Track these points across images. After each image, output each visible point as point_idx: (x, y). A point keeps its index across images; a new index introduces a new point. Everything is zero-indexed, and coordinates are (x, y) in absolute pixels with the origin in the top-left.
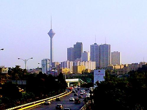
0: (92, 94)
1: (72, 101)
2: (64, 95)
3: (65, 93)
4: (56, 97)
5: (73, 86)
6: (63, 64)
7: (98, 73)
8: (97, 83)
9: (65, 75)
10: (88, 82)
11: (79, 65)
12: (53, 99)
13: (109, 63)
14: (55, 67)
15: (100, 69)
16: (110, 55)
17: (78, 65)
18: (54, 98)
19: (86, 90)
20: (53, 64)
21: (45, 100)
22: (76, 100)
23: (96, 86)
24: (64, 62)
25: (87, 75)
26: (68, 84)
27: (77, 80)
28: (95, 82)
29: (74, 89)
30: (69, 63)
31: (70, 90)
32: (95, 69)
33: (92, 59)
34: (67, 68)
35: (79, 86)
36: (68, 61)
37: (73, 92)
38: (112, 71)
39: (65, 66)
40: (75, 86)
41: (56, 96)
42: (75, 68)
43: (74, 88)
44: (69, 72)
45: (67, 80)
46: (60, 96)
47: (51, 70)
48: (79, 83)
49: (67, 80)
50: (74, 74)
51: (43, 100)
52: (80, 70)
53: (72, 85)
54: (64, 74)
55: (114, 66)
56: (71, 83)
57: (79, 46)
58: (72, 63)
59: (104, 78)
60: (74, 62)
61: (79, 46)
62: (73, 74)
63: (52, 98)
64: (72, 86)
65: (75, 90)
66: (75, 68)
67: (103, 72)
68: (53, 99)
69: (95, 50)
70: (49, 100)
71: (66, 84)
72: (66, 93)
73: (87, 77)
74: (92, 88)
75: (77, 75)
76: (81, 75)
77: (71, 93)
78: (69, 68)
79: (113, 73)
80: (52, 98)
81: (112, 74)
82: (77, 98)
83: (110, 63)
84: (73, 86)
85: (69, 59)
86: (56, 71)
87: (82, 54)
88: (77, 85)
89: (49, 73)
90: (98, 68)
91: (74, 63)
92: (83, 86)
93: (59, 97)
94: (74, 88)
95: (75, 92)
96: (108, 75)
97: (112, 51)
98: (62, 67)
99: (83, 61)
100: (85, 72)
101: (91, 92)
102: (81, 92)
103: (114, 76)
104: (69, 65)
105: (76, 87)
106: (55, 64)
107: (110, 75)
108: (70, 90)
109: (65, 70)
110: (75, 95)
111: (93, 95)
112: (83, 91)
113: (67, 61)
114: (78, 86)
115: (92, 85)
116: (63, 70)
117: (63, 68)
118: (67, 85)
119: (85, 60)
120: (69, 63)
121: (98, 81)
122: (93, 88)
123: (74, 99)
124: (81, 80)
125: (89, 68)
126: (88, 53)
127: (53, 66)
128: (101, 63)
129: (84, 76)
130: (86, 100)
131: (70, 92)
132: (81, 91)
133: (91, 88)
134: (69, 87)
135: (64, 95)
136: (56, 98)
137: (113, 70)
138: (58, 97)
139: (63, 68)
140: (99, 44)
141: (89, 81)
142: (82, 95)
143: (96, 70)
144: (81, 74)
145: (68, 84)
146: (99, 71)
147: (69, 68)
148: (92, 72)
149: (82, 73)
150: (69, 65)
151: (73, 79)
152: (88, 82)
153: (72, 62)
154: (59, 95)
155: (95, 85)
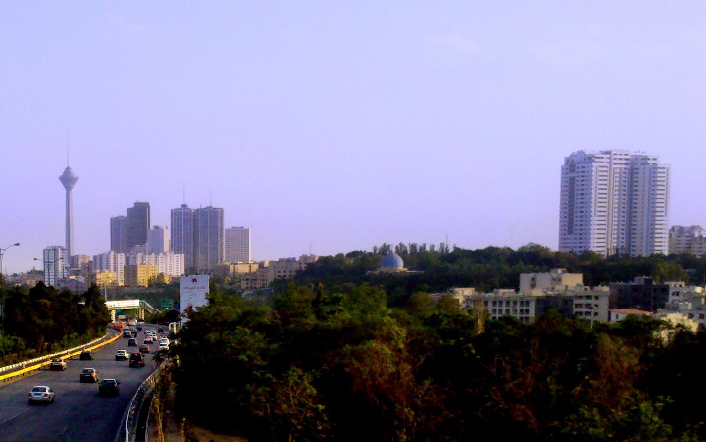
0: (176, 342)
1: (124, 358)
2: (101, 345)
3: (104, 337)
4: (82, 349)
5: (126, 320)
6: (100, 261)
7: (192, 284)
8: (189, 310)
9: (104, 290)
10: (164, 308)
11: (142, 264)
12: (74, 354)
13: (219, 257)
14: (78, 267)
15: (196, 274)
16: (221, 237)
17: (138, 264)
18: (74, 352)
19: (160, 331)
20: (73, 260)
21: (51, 358)
22: (132, 356)
23: (184, 320)
24: (101, 256)
25: (161, 291)
26: (113, 313)
27: (136, 303)
28: (183, 307)
29: (127, 327)
30: (115, 258)
31: (118, 329)
32: (183, 272)
33: (176, 248)
34: (110, 272)
35: (142, 321)
36: (112, 253)
37: (126, 336)
38: (228, 280)
39: (104, 265)
40: (131, 319)
41: (82, 346)
42: (131, 271)
43: (129, 325)
44: (114, 283)
45: (109, 304)
46: (92, 346)
47: (69, 275)
48: (140, 311)
49: (109, 304)
50: (128, 286)
51: (45, 357)
52: (143, 277)
53: (123, 317)
54: (101, 288)
55: (232, 267)
56: (123, 312)
57: (140, 212)
58: (121, 259)
59: (208, 299)
60: (128, 255)
61: (140, 212)
62: (125, 286)
63: (71, 353)
64: (122, 320)
65: (130, 329)
66: (131, 271)
67: (204, 281)
68: (74, 354)
69: (184, 222)
70: (63, 358)
71: (106, 312)
72: (107, 339)
73: (163, 295)
74: (174, 324)
75: (136, 290)
76: (147, 289)
77: (120, 338)
78: (115, 270)
79: (231, 284)
80: (71, 353)
81: (227, 287)
82: (136, 351)
83: (221, 258)
84: (126, 320)
85: (116, 246)
86: (81, 279)
87: (149, 234)
88: (137, 316)
89: (62, 285)
90: (191, 270)
91: (127, 259)
92: (153, 320)
93: (89, 349)
94: (129, 325)
95: (129, 337)
96: (218, 289)
97: (228, 223)
98: (96, 269)
99: (152, 252)
100: (157, 282)
101: (172, 337)
102: (146, 335)
103: (232, 292)
104: (115, 263)
105: (134, 322)
106: (79, 260)
107: (222, 289)
108: (118, 329)
109: (107, 277)
110: (131, 344)
111: (178, 344)
112: (152, 333)
113: (109, 253)
114: (140, 320)
115: (173, 316)
116: (98, 276)
117: (98, 271)
118: (111, 316)
119: (157, 250)
120: (115, 258)
121: (191, 307)
122: (177, 325)
123: (127, 355)
124: (146, 303)
125: (169, 270)
126: (165, 230)
127: (73, 266)
128: (200, 256)
129: (153, 291)
130: (159, 357)
131: (118, 337)
132: (145, 333)
133: (172, 326)
134: (114, 321)
135: (101, 345)
136: (79, 353)
137: (229, 276)
138: (86, 350)
139: (98, 271)
140: (193, 206)
141: (168, 307)
142: (150, 343)
143: (187, 276)
144: (147, 286)
145: (113, 313)
146: (194, 280)
147: (115, 270)
148: (176, 283)
149: (150, 285)
150: (115, 263)
151: (125, 301)
152: (164, 308)
153: (123, 254)
154: (88, 344)
155: (184, 316)
